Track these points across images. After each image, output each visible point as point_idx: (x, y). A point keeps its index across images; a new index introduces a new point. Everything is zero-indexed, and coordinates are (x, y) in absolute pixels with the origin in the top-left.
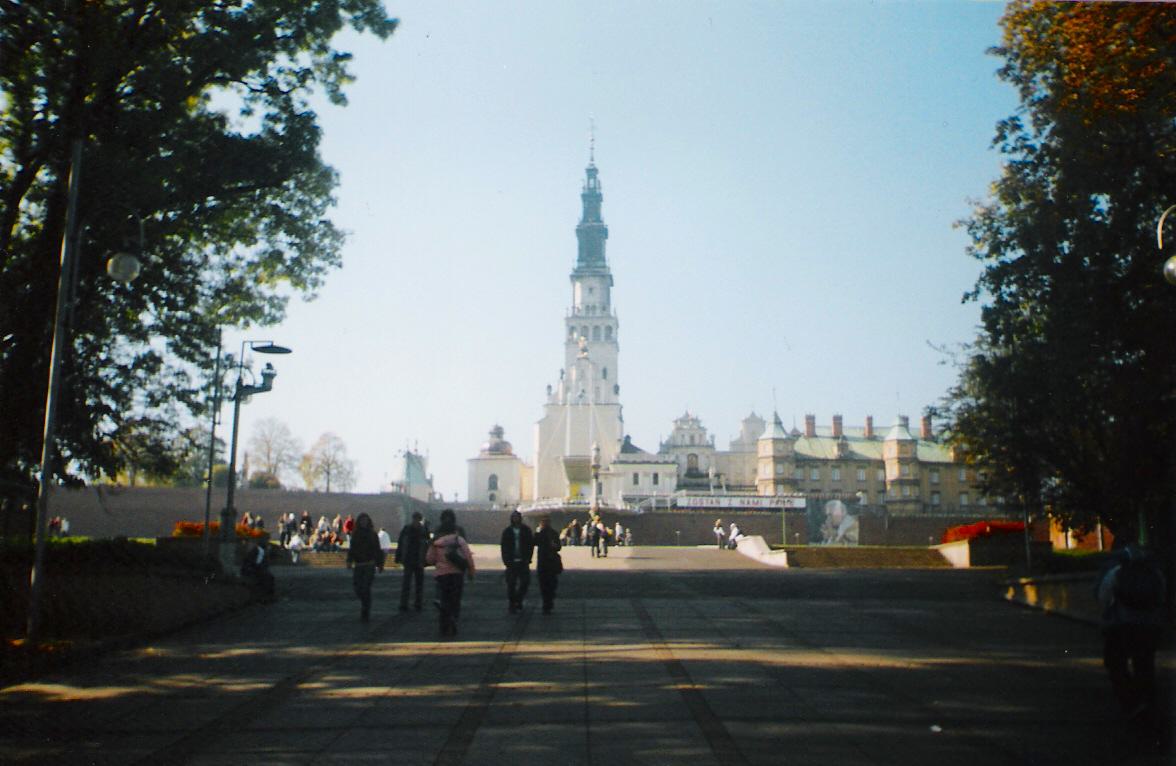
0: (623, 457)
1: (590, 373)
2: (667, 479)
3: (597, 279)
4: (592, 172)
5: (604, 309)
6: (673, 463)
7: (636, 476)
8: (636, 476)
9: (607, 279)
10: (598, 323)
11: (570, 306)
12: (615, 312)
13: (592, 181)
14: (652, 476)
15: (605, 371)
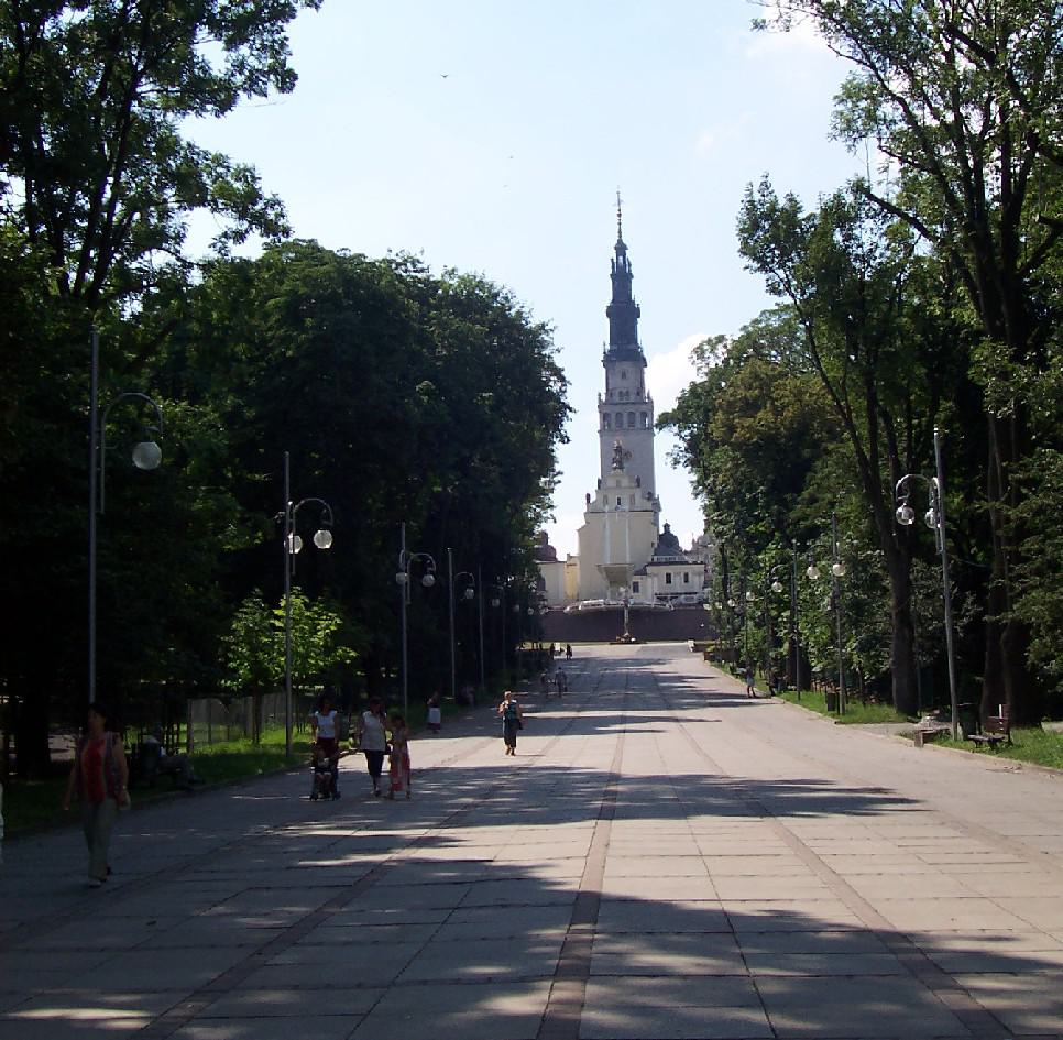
0: (655, 560)
1: (625, 482)
2: (697, 578)
3: (629, 363)
4: (621, 249)
5: (638, 394)
6: (702, 563)
7: (668, 576)
8: (668, 576)
9: (641, 362)
10: (632, 409)
11: (603, 391)
12: (649, 398)
13: (621, 258)
14: (682, 575)
15: (638, 481)
